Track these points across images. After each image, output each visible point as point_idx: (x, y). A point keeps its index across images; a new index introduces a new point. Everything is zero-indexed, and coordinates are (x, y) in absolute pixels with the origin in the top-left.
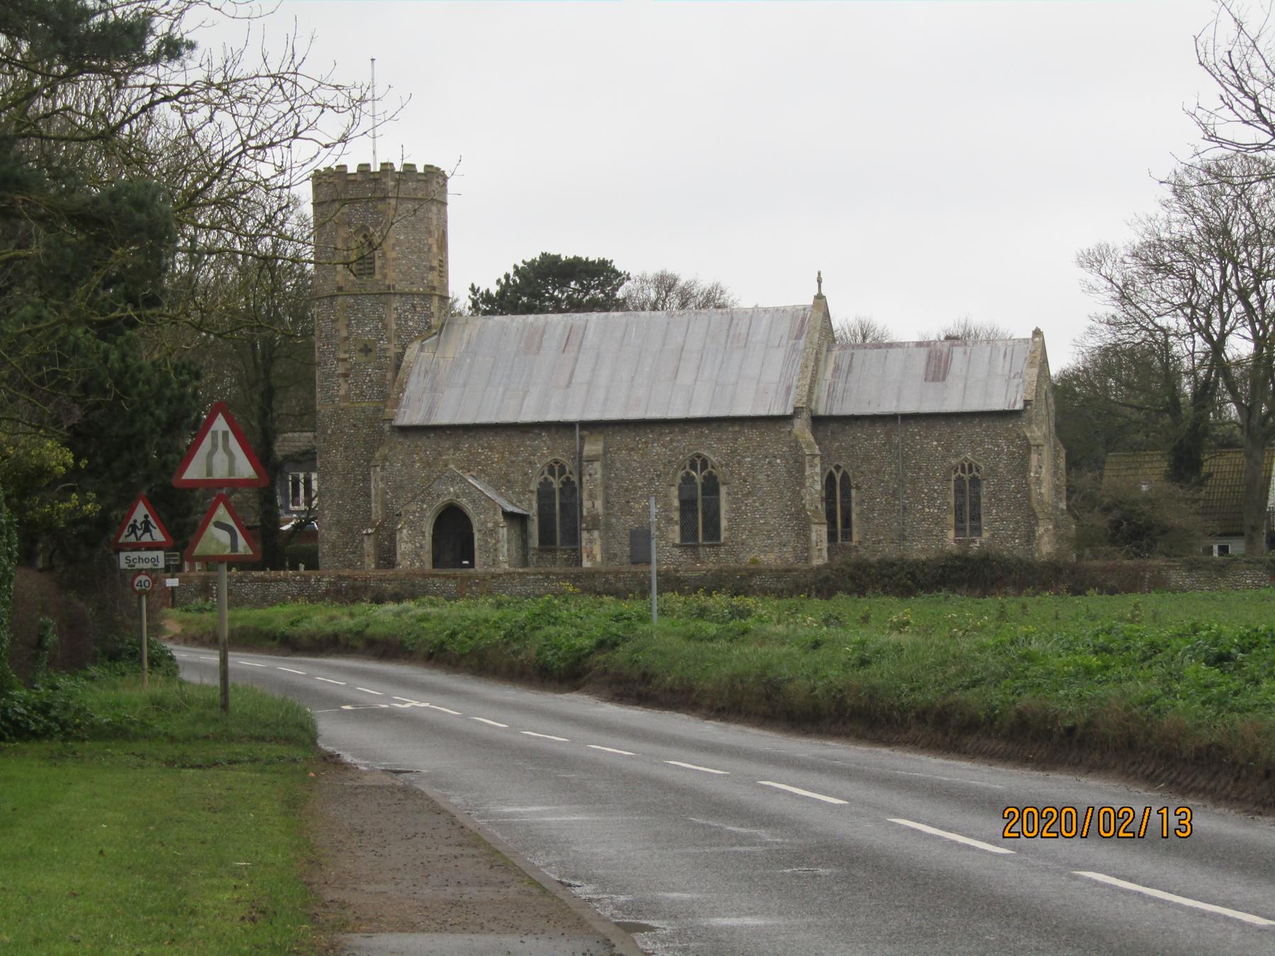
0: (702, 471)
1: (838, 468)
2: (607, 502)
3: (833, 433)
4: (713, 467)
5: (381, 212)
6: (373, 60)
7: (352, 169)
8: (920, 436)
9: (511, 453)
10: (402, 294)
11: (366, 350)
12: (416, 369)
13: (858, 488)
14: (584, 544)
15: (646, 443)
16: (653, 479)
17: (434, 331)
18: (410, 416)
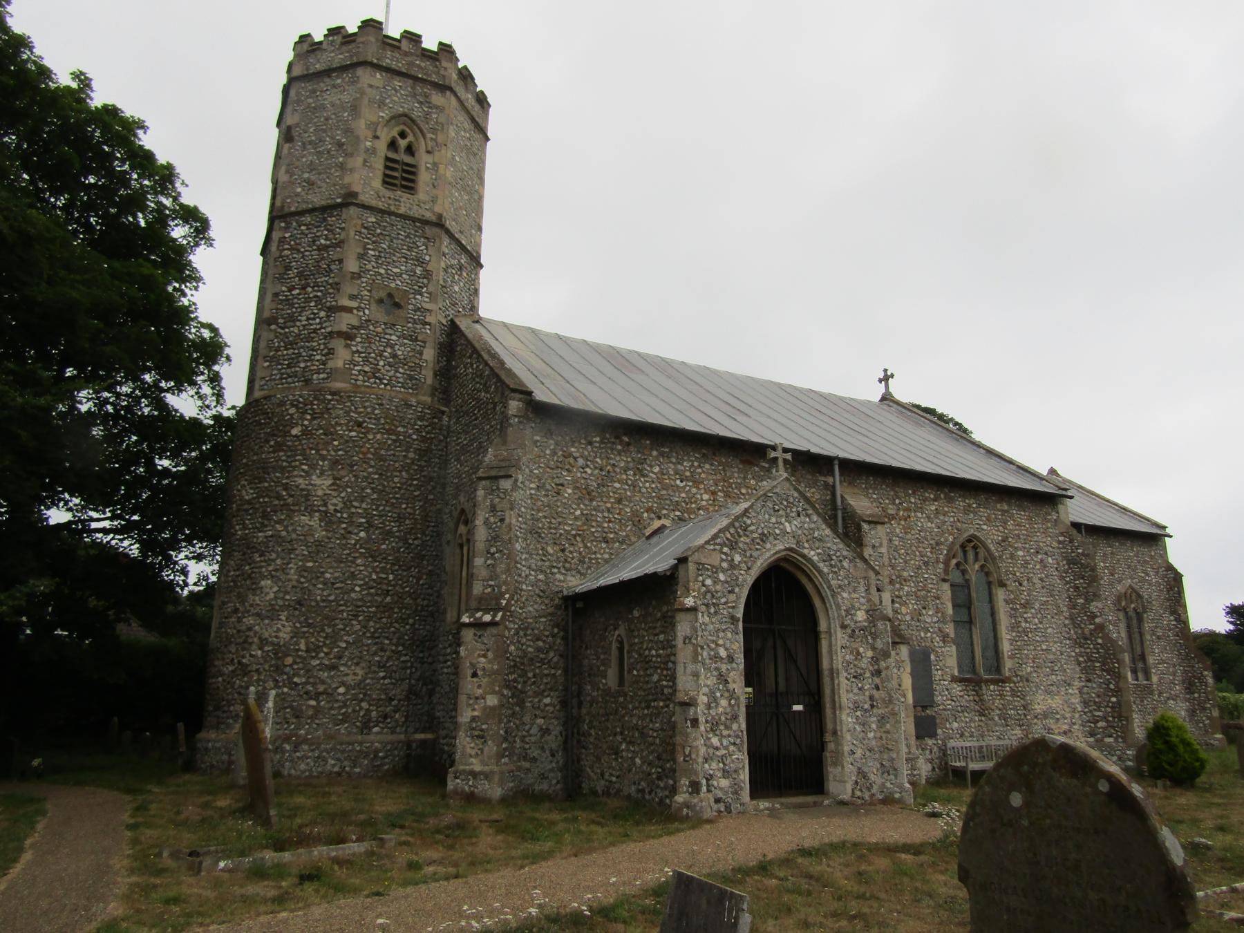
5: (437, 107)
11: (393, 302)
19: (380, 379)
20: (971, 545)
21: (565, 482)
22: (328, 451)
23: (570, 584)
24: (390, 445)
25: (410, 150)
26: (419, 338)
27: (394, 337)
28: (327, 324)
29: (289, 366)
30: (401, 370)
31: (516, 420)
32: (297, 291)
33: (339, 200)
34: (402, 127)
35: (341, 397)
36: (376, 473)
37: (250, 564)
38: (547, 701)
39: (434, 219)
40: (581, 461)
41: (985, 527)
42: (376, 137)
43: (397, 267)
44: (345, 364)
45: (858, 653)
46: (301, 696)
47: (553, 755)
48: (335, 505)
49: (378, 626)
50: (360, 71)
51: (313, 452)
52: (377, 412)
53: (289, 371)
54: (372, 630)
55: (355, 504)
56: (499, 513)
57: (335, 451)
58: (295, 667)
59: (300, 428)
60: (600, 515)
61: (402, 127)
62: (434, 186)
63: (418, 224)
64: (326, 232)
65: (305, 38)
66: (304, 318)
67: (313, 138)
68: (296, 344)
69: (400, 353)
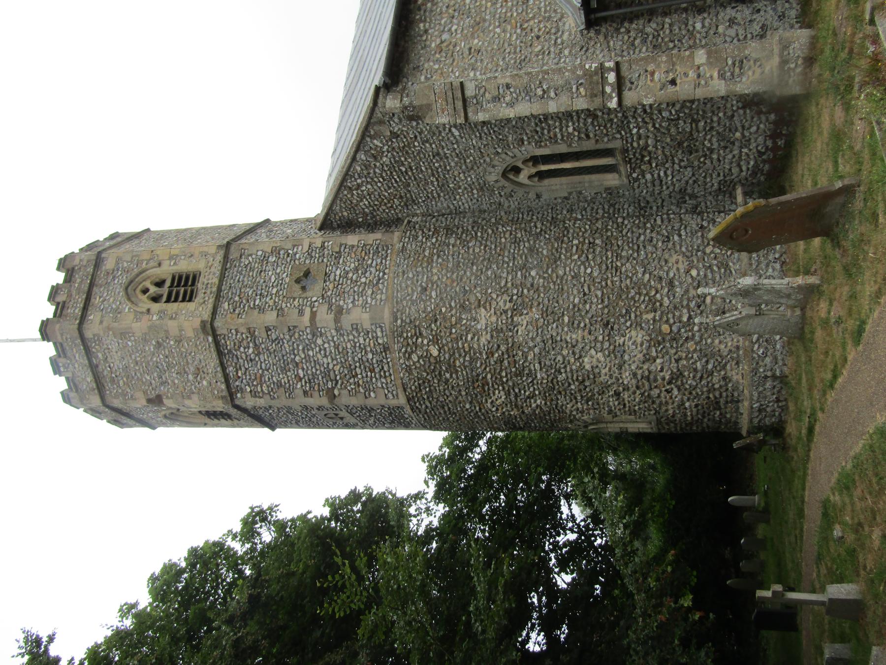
5: (117, 263)
11: (304, 278)
19: (379, 280)
21: (467, 47)
22: (452, 316)
23: (573, 25)
24: (443, 260)
25: (160, 284)
26: (337, 250)
27: (338, 273)
28: (328, 335)
29: (372, 370)
30: (370, 262)
31: (405, 99)
32: (300, 371)
33: (210, 339)
34: (138, 291)
35: (398, 311)
36: (472, 269)
37: (570, 385)
38: (698, 26)
39: (222, 252)
40: (445, 36)
42: (148, 310)
43: (270, 279)
44: (366, 312)
46: (702, 312)
47: (758, 11)
48: (505, 302)
49: (626, 248)
50: (88, 334)
51: (454, 331)
52: (411, 275)
53: (377, 370)
54: (631, 252)
55: (503, 284)
56: (501, 91)
57: (451, 310)
58: (672, 321)
59: (431, 347)
60: (499, 11)
61: (138, 291)
62: (192, 256)
63: (229, 265)
64: (242, 349)
65: (66, 398)
66: (325, 360)
67: (155, 375)
68: (350, 365)
69: (353, 265)
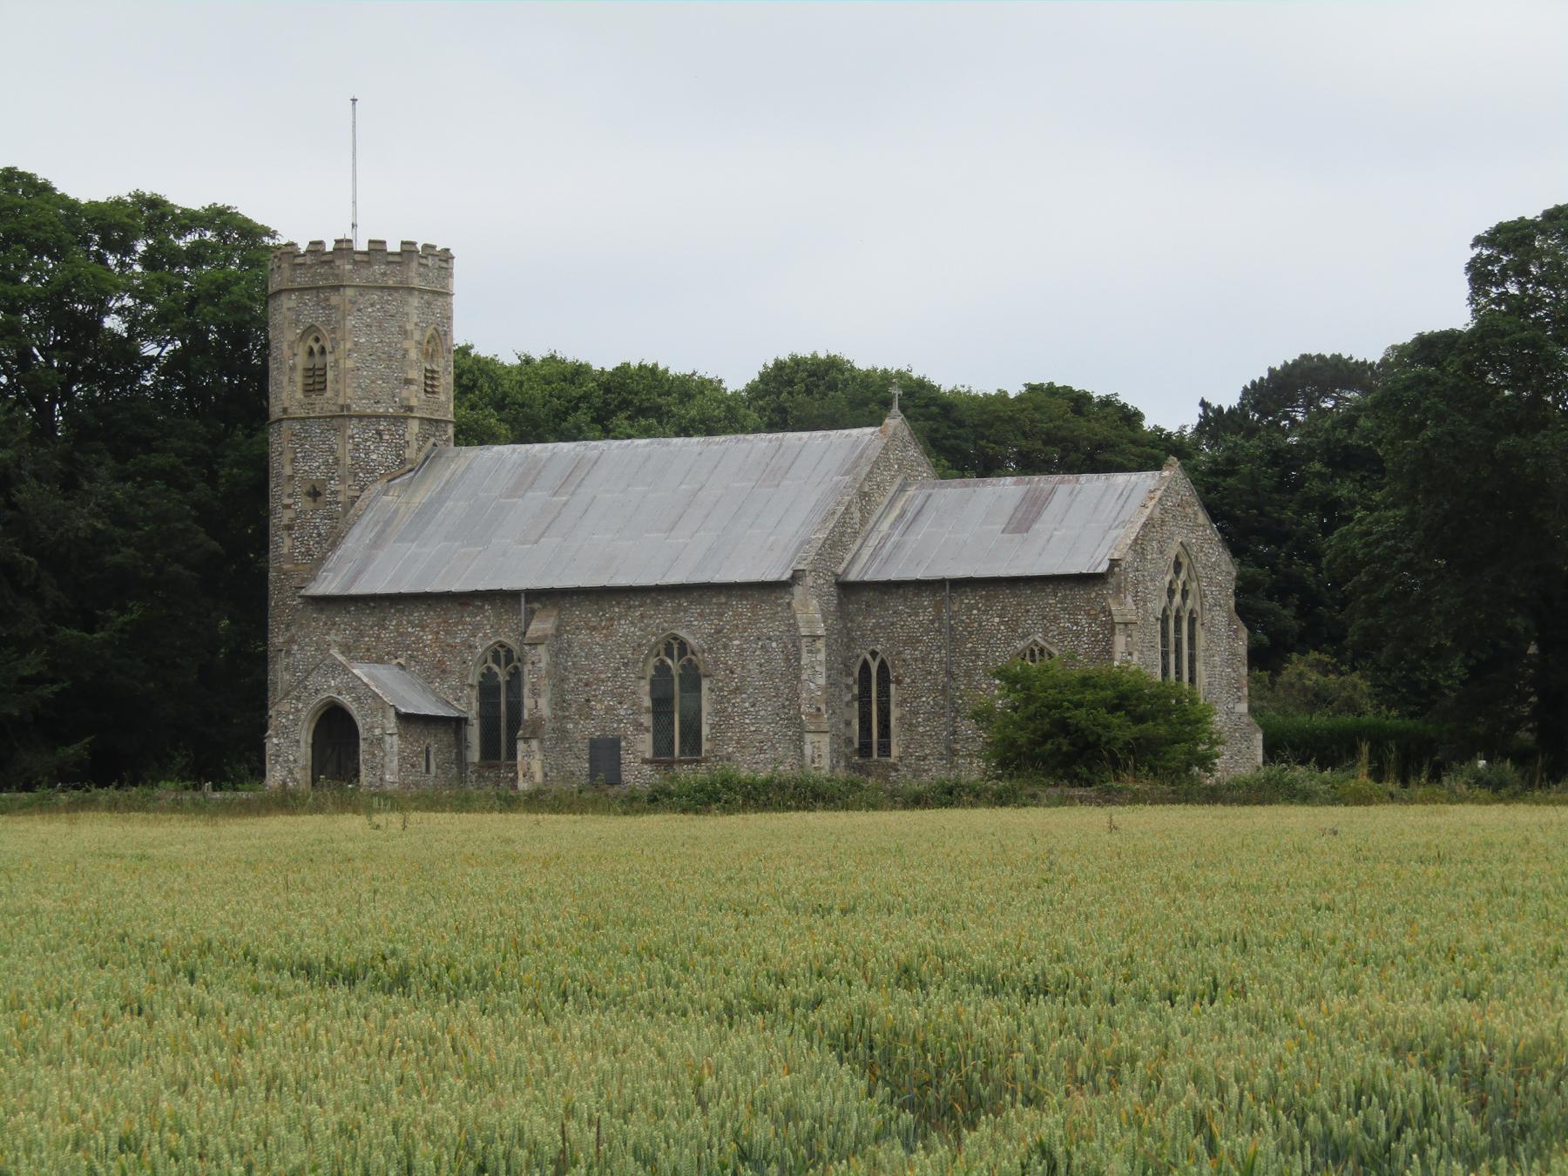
0: (680, 658)
1: (874, 654)
2: (560, 703)
3: (868, 606)
4: (693, 653)
5: (334, 307)
6: (354, 100)
7: (303, 247)
8: (979, 609)
9: (447, 633)
10: (360, 417)
12: (366, 519)
13: (899, 682)
14: (519, 758)
15: (611, 619)
16: (619, 669)
17: (409, 466)
18: (328, 584)
20: (673, 646)
25: (323, 351)
34: (315, 334)
40: (342, 626)
41: (696, 623)
42: (295, 355)
45: (374, 754)
61: (315, 334)
62: (337, 382)
